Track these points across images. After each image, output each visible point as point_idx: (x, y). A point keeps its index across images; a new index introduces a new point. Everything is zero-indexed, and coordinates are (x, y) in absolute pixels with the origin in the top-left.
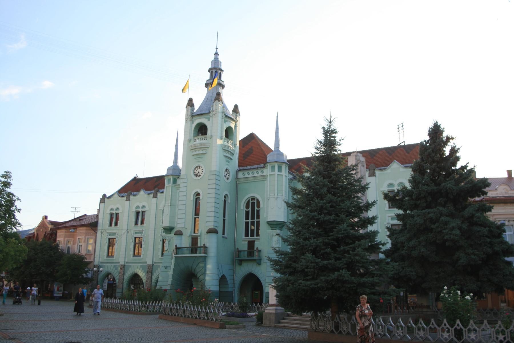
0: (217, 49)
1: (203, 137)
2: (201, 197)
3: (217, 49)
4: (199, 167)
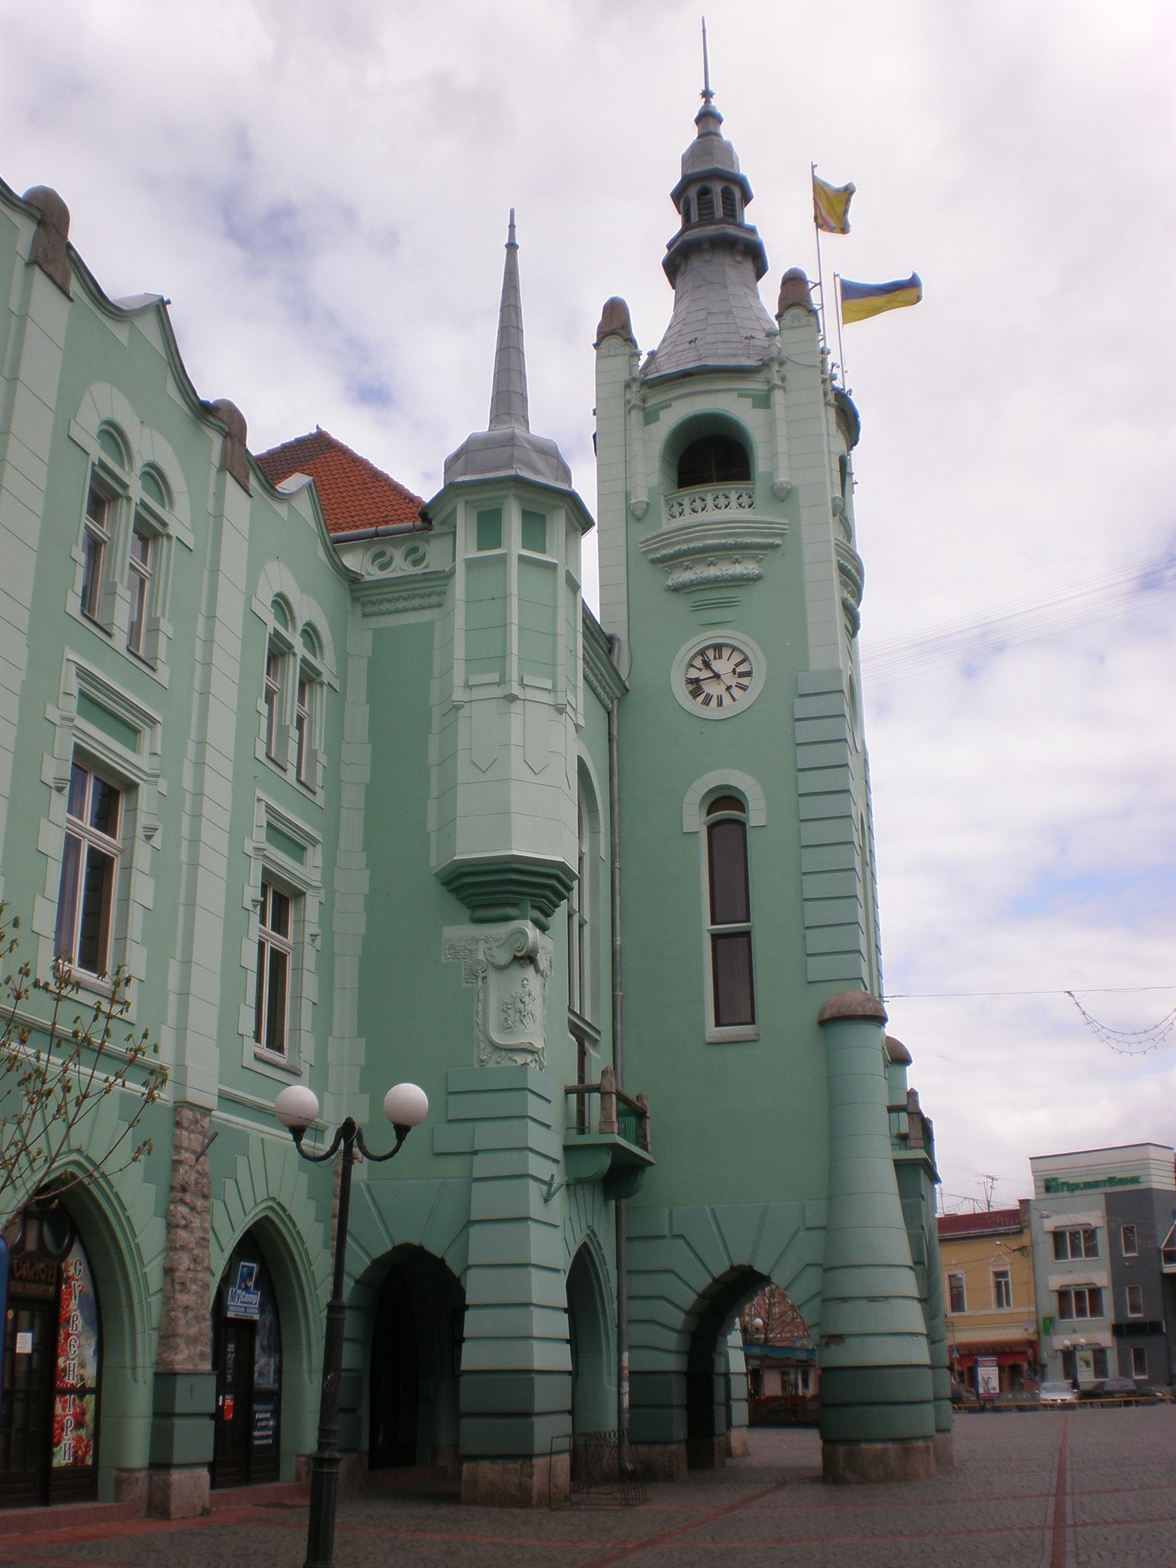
0: (707, 94)
1: (733, 490)
2: (756, 815)
3: (707, 94)
4: (718, 648)
